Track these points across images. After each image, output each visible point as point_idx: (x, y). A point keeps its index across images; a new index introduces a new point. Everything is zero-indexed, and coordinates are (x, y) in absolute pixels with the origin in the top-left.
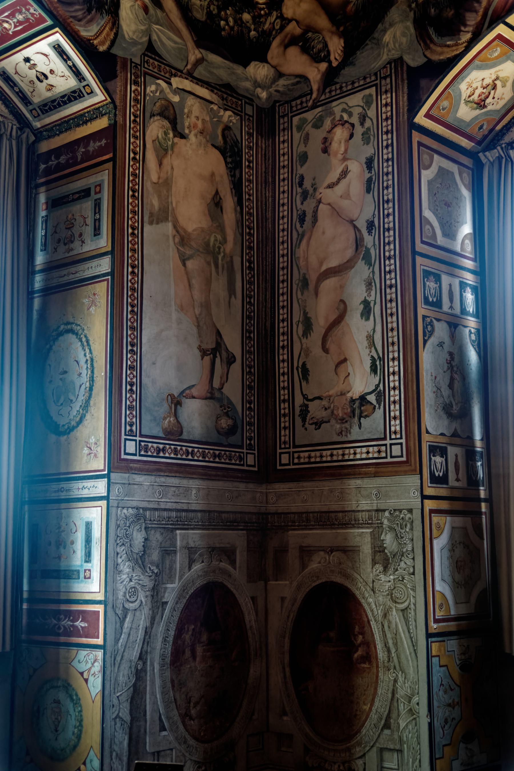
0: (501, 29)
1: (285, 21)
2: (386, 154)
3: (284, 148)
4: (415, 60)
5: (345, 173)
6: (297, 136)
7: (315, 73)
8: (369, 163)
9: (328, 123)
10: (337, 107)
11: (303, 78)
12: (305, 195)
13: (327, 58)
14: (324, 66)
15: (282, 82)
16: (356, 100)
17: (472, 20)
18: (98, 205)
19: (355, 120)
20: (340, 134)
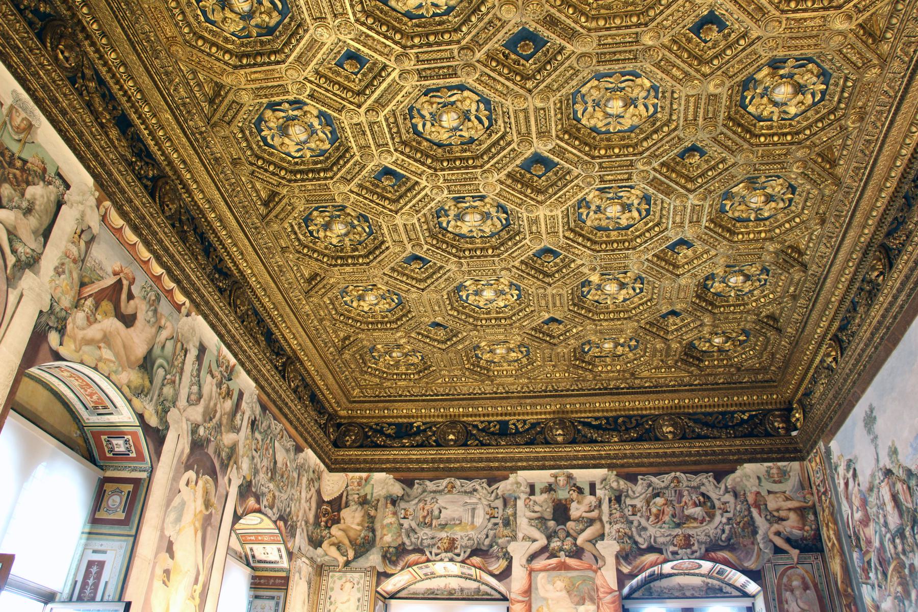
0: (410, 569)
1: (331, 536)
2: (366, 598)
3: (324, 582)
4: (381, 570)
5: (349, 600)
6: (330, 580)
7: (342, 560)
8: (359, 600)
9: (344, 580)
10: (349, 575)
11: (336, 559)
12: (331, 603)
13: (347, 556)
14: (345, 558)
15: (327, 558)
16: (356, 575)
17: (402, 564)
18: (277, 604)
19: (355, 582)
20: (349, 585)
